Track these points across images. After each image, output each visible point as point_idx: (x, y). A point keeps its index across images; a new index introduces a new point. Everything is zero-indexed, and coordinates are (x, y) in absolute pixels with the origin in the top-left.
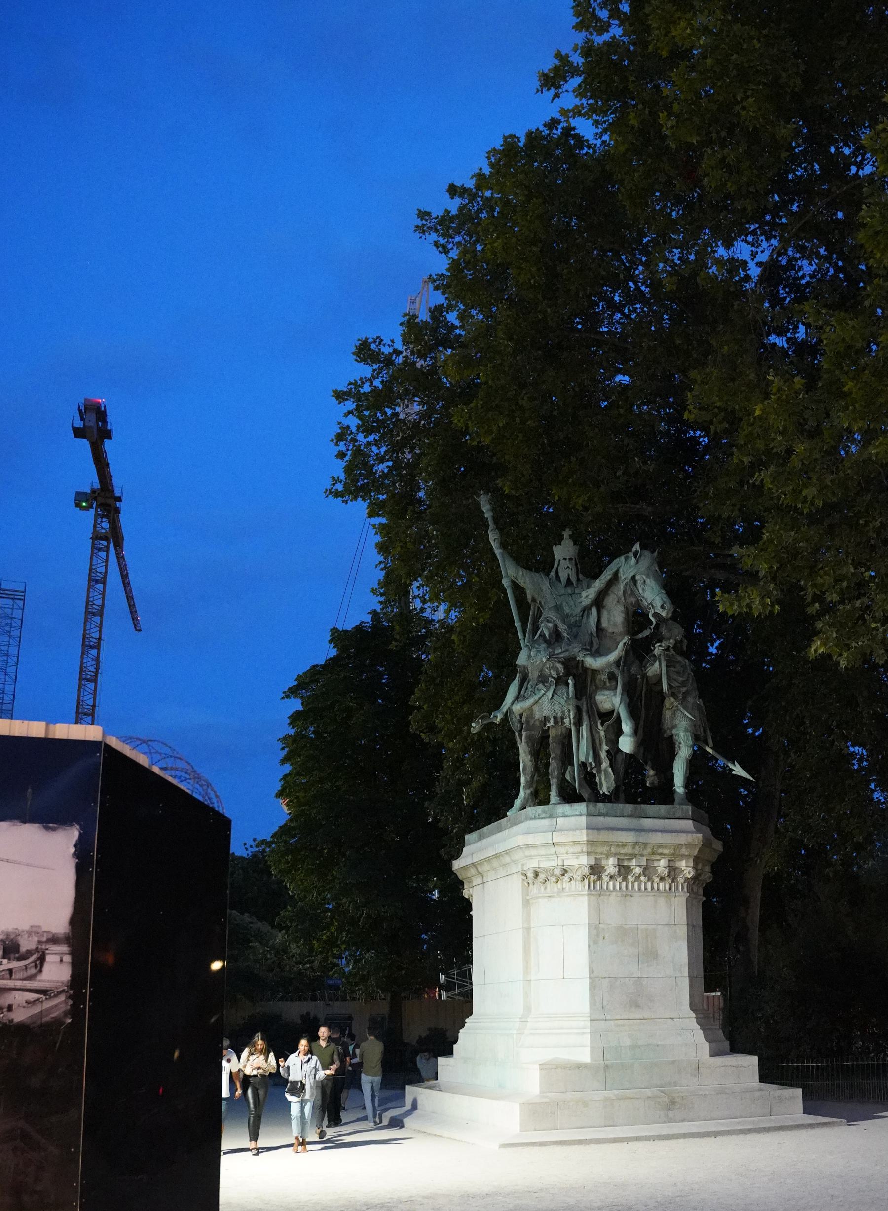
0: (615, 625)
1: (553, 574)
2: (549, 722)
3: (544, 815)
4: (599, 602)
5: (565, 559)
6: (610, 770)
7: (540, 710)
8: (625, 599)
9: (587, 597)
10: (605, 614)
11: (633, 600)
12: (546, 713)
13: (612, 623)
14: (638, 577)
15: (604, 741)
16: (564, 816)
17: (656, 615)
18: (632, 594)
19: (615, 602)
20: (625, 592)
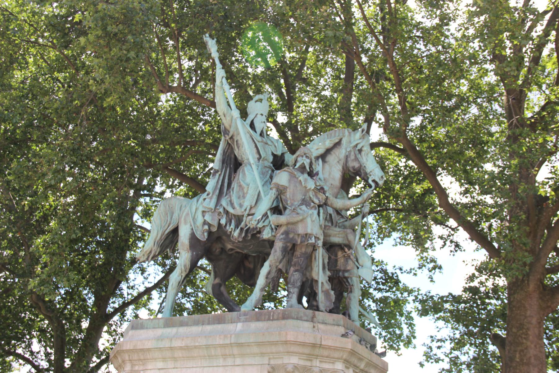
0: (334, 179)
1: (249, 120)
2: (311, 239)
3: (305, 318)
4: (323, 157)
5: (262, 115)
6: (332, 293)
7: (306, 227)
8: (347, 161)
9: (317, 149)
10: (327, 166)
11: (356, 165)
12: (309, 231)
13: (331, 176)
14: (364, 149)
15: (327, 267)
16: (324, 323)
17: (374, 181)
18: (356, 159)
19: (336, 161)
20: (347, 157)
